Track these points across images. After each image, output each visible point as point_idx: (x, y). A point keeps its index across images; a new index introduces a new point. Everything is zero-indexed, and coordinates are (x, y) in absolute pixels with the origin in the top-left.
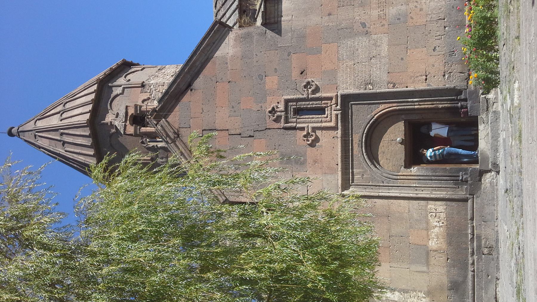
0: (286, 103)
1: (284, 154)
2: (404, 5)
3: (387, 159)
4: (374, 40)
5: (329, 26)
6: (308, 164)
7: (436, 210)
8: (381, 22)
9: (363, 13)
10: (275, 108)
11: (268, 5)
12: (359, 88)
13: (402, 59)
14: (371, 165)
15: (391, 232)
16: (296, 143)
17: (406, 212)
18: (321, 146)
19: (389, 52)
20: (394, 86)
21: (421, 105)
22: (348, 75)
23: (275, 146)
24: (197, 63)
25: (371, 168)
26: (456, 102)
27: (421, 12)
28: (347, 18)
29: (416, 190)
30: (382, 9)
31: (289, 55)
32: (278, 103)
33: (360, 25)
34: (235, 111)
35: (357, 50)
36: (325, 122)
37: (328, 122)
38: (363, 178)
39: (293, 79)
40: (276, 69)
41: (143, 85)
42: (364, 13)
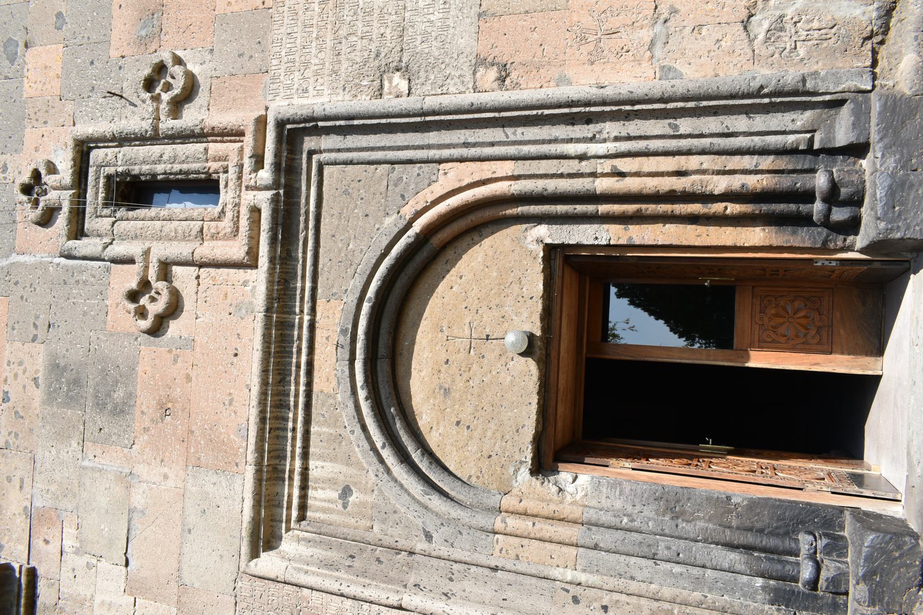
0: (82, 151)
1: (62, 364)
3: (458, 423)
6: (137, 413)
10: (43, 172)
12: (351, 87)
14: (383, 447)
16: (105, 323)
18: (191, 343)
20: (502, 80)
21: (622, 175)
22: (315, 30)
23: (35, 325)
26: (804, 162)
36: (214, 237)
37: (226, 238)
38: (345, 507)
39: (114, 54)
40: (59, 15)
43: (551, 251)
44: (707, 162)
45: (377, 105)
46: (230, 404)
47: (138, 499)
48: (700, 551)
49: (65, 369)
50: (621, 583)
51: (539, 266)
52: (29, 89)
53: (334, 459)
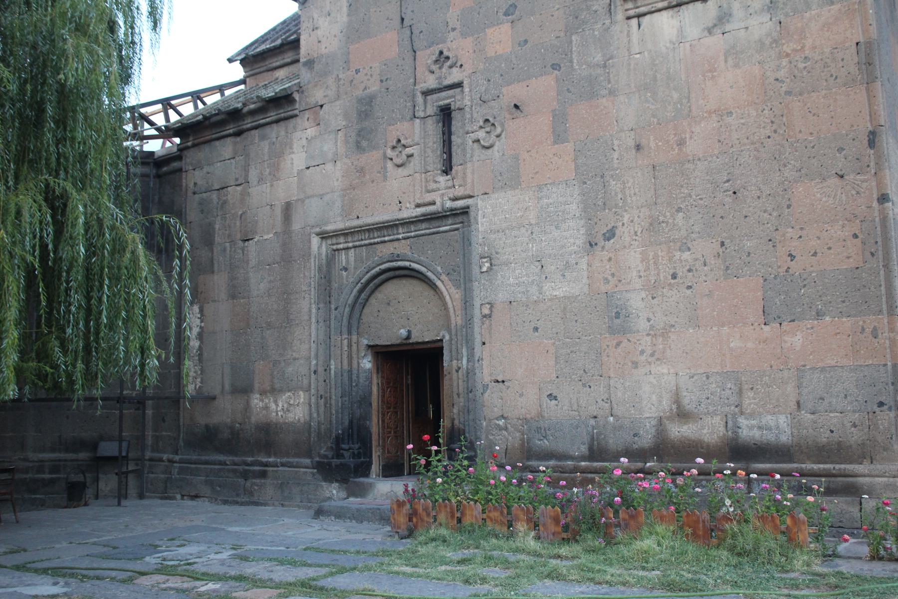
2: (648, 324)
4: (577, 264)
5: (612, 152)
8: (613, 275)
9: (636, 229)
10: (449, 63)
15: (268, 329)
17: (294, 354)
19: (550, 300)
20: (485, 316)
25: (357, 284)
27: (630, 364)
28: (627, 192)
29: (325, 370)
30: (642, 274)
31: (555, 67)
32: (461, 66)
33: (610, 227)
35: (557, 227)
36: (427, 181)
37: (426, 186)
38: (341, 270)
40: (526, 41)
42: (636, 232)
43: (441, 340)
46: (366, 207)
47: (329, 166)
49: (371, 106)
50: (333, 386)
52: (489, 31)
53: (355, 261)
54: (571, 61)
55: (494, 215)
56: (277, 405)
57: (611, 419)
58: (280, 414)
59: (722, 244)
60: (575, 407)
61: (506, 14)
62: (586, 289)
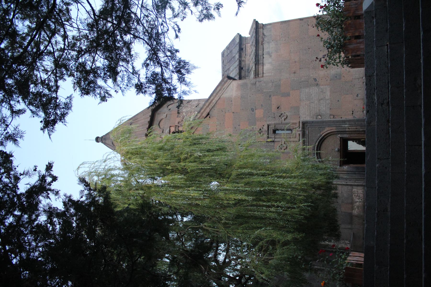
7: (357, 192)
8: (326, 78)
10: (262, 129)
11: (257, 66)
13: (338, 101)
20: (333, 117)
24: (214, 101)
29: (346, 180)
31: (270, 96)
34: (237, 131)
35: (311, 95)
39: (273, 111)
41: (178, 113)
43: (340, 138)
44: (359, 127)
45: (317, 120)
48: (361, 173)
51: (339, 140)
52: (256, 116)
54: (270, 92)
55: (306, 114)
56: (357, 202)
57: (364, 78)
58: (360, 201)
59: (321, 51)
60: (360, 88)
61: (253, 111)
62: (329, 86)
